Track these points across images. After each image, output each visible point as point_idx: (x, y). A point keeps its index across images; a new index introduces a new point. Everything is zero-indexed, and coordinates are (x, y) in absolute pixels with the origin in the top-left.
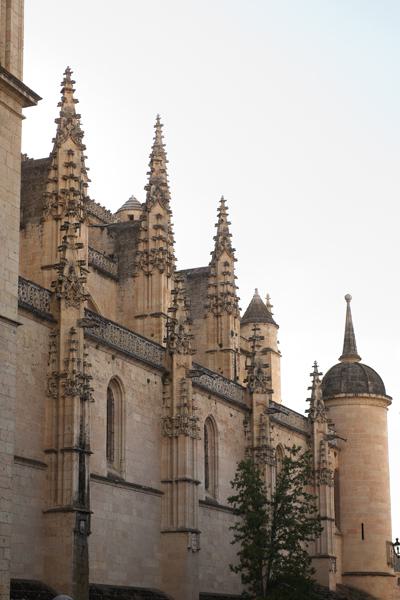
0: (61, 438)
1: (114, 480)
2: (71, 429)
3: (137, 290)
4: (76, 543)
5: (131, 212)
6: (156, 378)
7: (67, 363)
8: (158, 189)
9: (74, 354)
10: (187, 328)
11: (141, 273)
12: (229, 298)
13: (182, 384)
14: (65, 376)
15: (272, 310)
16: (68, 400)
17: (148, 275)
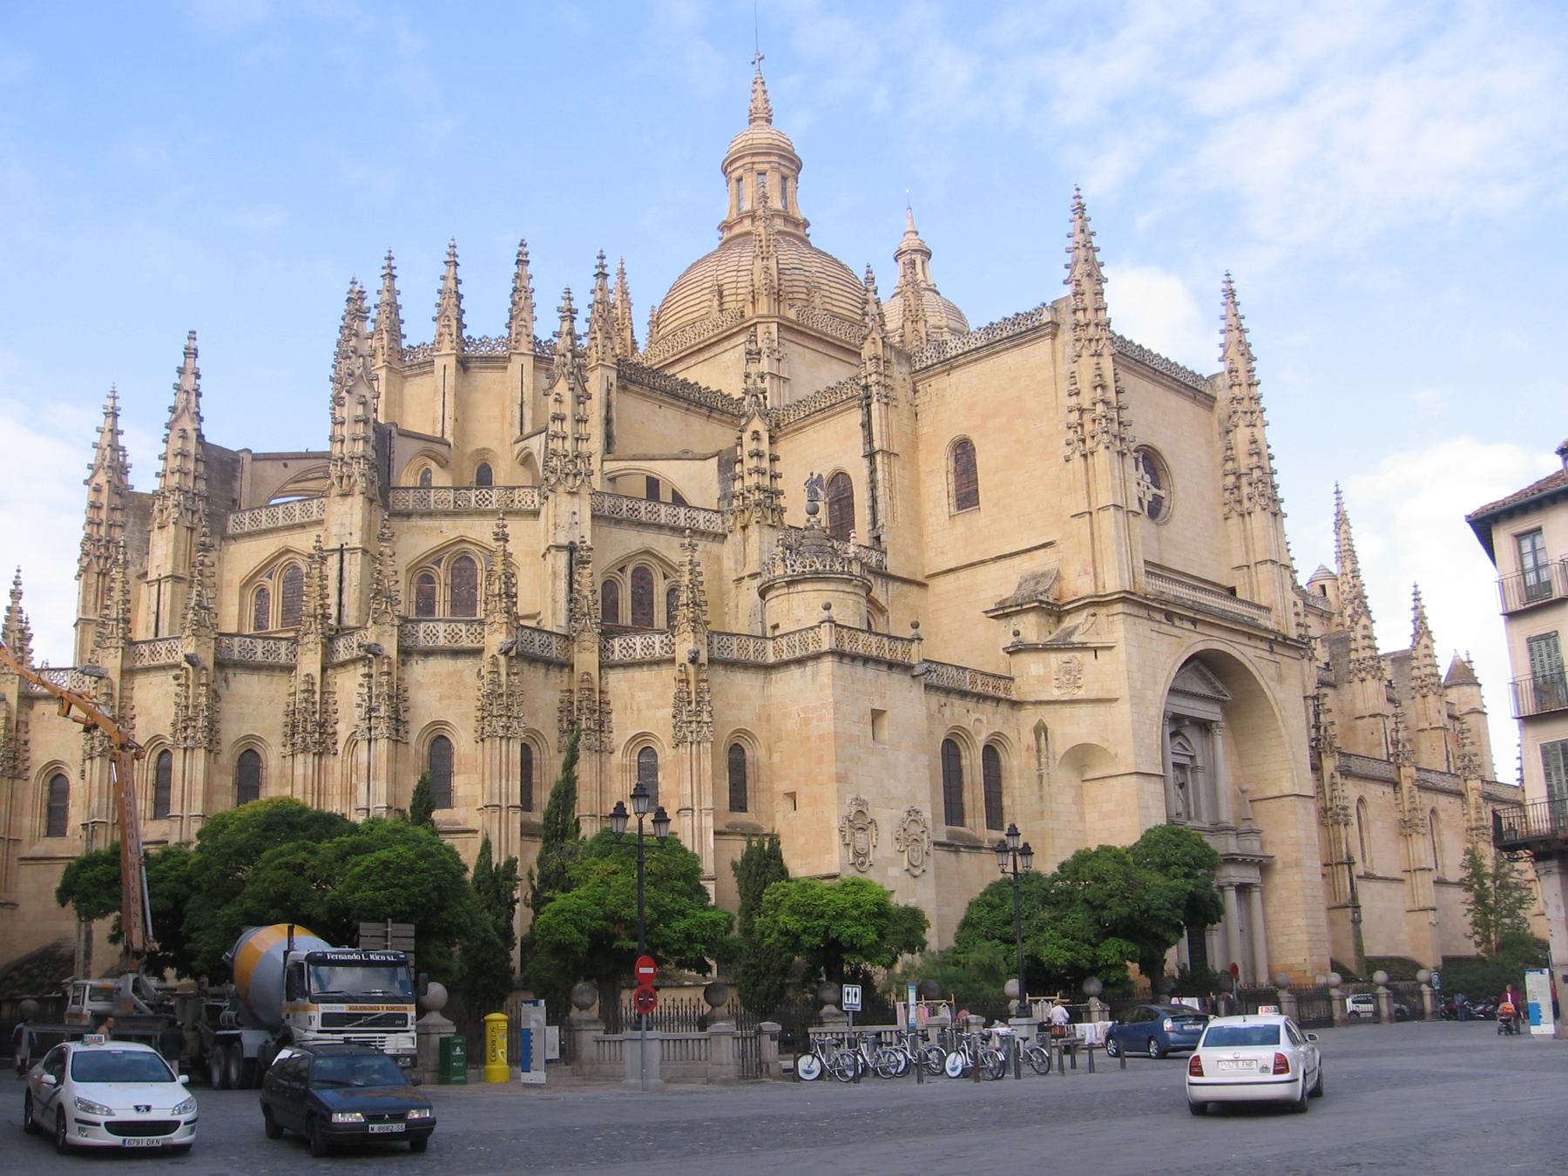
0: (1334, 855)
1: (1369, 877)
2: (1340, 847)
3: (1353, 694)
4: (1354, 929)
5: (1322, 583)
6: (1389, 790)
7: (1331, 800)
8: (1346, 553)
9: (1336, 793)
10: (1408, 746)
11: (1356, 679)
12: (1433, 680)
13: (1410, 791)
14: (1331, 809)
15: (1474, 665)
16: (1336, 826)
17: (1363, 680)
